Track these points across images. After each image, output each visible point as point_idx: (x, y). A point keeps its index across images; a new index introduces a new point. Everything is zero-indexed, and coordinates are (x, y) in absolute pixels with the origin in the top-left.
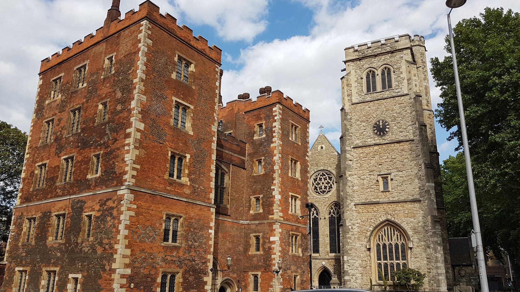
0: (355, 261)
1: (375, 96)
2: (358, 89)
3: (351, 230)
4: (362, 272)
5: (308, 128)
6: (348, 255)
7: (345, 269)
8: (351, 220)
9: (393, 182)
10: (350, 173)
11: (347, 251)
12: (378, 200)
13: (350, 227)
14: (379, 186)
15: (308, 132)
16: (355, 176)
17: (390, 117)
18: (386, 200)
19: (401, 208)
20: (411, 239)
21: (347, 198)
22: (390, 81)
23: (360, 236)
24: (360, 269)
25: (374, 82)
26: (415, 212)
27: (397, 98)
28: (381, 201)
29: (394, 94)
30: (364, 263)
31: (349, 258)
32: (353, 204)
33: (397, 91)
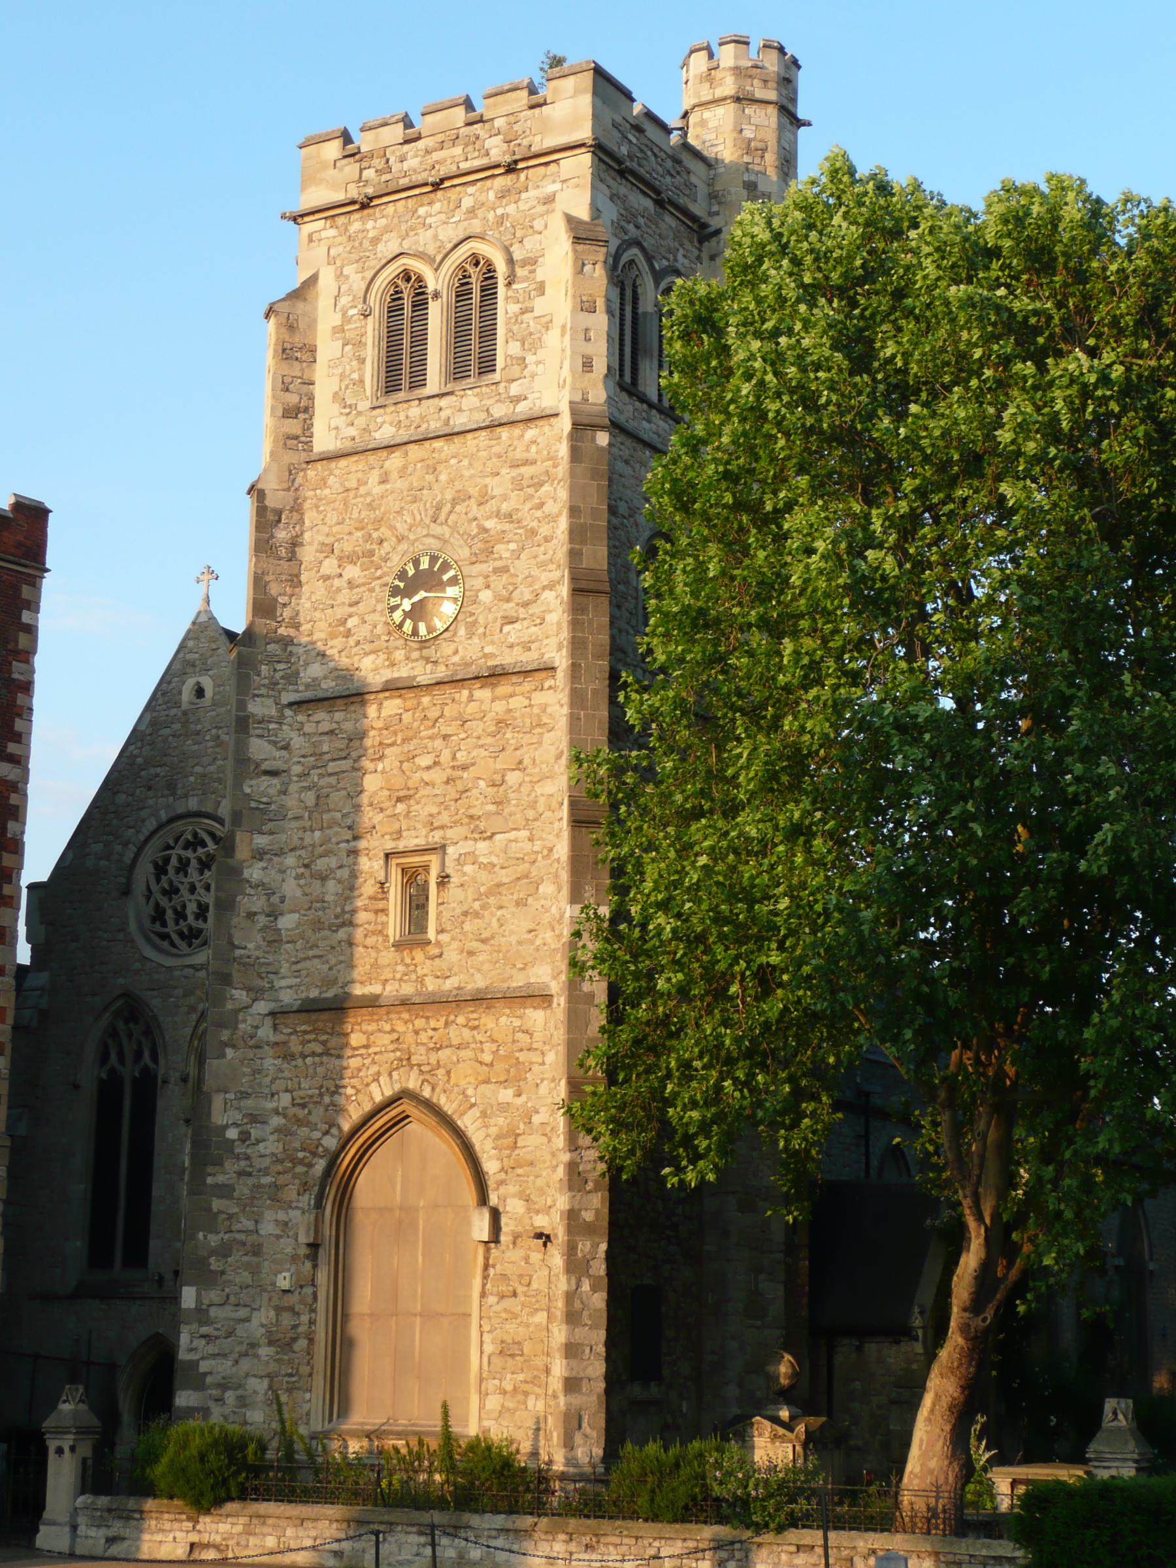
0: (242, 1313)
1: (414, 413)
2: (342, 376)
3: (239, 1149)
4: (273, 1367)
5: (33, 606)
6: (206, 1278)
7: (183, 1355)
8: (245, 1095)
9: (453, 892)
10: (261, 841)
11: (203, 1263)
12: (376, 989)
13: (232, 1134)
14: (384, 911)
15: (31, 630)
16: (290, 860)
17: (468, 537)
18: (408, 989)
19: (466, 1033)
20: (493, 1199)
21: (226, 979)
22: (488, 333)
23: (282, 1179)
24: (265, 1351)
25: (420, 339)
26: (522, 1057)
27: (504, 433)
28: (390, 991)
29: (500, 411)
30: (287, 1320)
31: (214, 1295)
32: (262, 1007)
33: (515, 389)
